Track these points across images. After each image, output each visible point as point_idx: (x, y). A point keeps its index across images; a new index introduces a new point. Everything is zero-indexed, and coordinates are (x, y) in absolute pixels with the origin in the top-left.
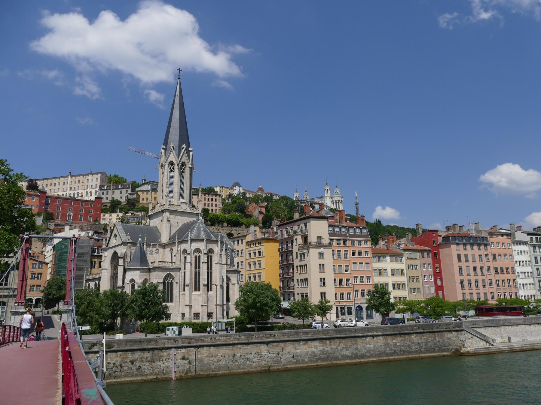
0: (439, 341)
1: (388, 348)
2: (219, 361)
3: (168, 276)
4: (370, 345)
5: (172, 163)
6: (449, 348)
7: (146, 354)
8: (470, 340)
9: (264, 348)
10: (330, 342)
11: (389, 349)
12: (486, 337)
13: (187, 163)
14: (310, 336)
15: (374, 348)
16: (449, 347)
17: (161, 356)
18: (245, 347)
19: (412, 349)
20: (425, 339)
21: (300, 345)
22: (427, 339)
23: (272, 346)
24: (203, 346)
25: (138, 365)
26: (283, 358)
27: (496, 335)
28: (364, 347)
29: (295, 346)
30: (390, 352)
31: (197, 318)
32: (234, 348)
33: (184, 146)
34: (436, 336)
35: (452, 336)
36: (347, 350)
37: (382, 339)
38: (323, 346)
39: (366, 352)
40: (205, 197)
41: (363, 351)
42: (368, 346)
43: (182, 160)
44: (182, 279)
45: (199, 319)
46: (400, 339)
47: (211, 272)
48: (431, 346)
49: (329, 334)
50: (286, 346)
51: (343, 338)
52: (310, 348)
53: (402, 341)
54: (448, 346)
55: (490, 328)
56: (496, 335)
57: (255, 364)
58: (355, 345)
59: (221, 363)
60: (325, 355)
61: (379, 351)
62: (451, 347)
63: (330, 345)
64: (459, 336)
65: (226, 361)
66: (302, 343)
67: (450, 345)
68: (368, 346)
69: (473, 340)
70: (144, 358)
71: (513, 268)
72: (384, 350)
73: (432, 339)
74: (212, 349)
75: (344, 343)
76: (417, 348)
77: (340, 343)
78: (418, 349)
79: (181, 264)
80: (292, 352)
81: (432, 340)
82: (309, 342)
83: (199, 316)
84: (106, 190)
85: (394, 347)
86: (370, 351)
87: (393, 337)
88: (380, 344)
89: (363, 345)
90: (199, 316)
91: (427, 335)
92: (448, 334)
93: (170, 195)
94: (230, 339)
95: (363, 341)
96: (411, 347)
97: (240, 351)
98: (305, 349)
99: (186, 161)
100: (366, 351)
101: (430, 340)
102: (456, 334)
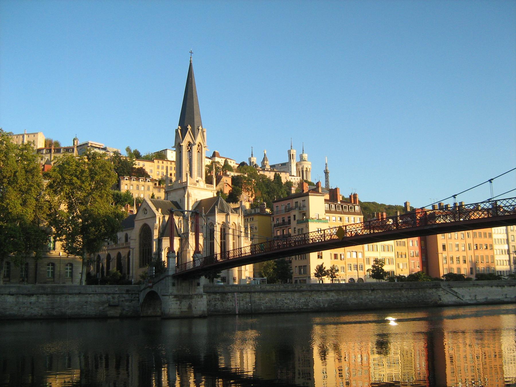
7: (218, 296)
9: (296, 295)
12: (458, 294)
17: (228, 298)
18: (283, 294)
20: (412, 293)
24: (254, 292)
25: (213, 303)
36: (355, 299)
37: (380, 292)
40: (158, 164)
42: (370, 297)
44: (209, 249)
49: (342, 287)
51: (352, 290)
57: (291, 306)
59: (268, 304)
61: (378, 301)
63: (343, 296)
65: (271, 303)
66: (323, 293)
68: (370, 297)
70: (217, 299)
71: (491, 246)
72: (381, 300)
74: (262, 295)
79: (208, 235)
81: (417, 294)
82: (328, 293)
83: (225, 280)
84: (46, 153)
85: (389, 298)
91: (414, 291)
94: (273, 288)
97: (281, 297)
100: (368, 300)
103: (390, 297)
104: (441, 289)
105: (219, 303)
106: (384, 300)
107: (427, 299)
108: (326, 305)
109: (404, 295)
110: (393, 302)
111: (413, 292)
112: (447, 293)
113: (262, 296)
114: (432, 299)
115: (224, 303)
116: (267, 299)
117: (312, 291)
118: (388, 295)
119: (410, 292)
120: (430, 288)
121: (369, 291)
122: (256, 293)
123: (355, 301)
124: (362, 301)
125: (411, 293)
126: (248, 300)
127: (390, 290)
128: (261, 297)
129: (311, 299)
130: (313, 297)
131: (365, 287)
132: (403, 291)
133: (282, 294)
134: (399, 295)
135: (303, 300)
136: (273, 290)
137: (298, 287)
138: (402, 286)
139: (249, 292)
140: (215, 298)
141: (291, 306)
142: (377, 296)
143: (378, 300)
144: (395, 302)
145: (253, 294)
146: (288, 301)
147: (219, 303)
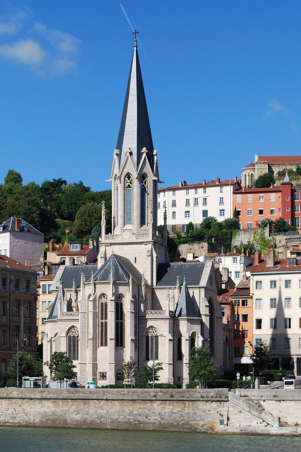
0: (188, 413)
4: (102, 410)
5: (129, 176)
6: (199, 424)
8: (237, 416)
10: (63, 403)
11: (122, 417)
14: (45, 395)
15: (106, 414)
16: (199, 422)
21: (35, 404)
22: (173, 409)
23: (12, 403)
28: (95, 411)
29: (29, 404)
30: (123, 420)
34: (187, 406)
36: (78, 413)
37: (118, 404)
39: (96, 418)
42: (100, 411)
46: (139, 406)
48: (176, 419)
49: (63, 395)
50: (23, 404)
52: (43, 408)
53: (140, 408)
54: (198, 421)
58: (86, 409)
60: (55, 416)
61: (111, 418)
62: (203, 423)
63: (63, 407)
64: (219, 409)
68: (100, 411)
69: (242, 414)
72: (117, 417)
73: (180, 410)
75: (76, 406)
76: (155, 420)
77: (72, 405)
78: (157, 420)
81: (179, 411)
82: (43, 402)
85: (129, 415)
86: (102, 417)
87: (131, 402)
88: (114, 411)
89: (96, 410)
90: (106, 376)
91: (175, 405)
95: (96, 406)
98: (39, 408)
99: (130, 172)
102: (216, 406)
103: (131, 413)
106: (121, 417)
107: (197, 421)
108: (37, 420)
109: (156, 411)
112: (241, 412)
119: (167, 407)
123: (78, 417)
124: (87, 416)
129: (21, 410)
131: (95, 395)
135: (10, 411)
137: (7, 393)
142: (112, 410)
143: (112, 417)
144: (136, 422)
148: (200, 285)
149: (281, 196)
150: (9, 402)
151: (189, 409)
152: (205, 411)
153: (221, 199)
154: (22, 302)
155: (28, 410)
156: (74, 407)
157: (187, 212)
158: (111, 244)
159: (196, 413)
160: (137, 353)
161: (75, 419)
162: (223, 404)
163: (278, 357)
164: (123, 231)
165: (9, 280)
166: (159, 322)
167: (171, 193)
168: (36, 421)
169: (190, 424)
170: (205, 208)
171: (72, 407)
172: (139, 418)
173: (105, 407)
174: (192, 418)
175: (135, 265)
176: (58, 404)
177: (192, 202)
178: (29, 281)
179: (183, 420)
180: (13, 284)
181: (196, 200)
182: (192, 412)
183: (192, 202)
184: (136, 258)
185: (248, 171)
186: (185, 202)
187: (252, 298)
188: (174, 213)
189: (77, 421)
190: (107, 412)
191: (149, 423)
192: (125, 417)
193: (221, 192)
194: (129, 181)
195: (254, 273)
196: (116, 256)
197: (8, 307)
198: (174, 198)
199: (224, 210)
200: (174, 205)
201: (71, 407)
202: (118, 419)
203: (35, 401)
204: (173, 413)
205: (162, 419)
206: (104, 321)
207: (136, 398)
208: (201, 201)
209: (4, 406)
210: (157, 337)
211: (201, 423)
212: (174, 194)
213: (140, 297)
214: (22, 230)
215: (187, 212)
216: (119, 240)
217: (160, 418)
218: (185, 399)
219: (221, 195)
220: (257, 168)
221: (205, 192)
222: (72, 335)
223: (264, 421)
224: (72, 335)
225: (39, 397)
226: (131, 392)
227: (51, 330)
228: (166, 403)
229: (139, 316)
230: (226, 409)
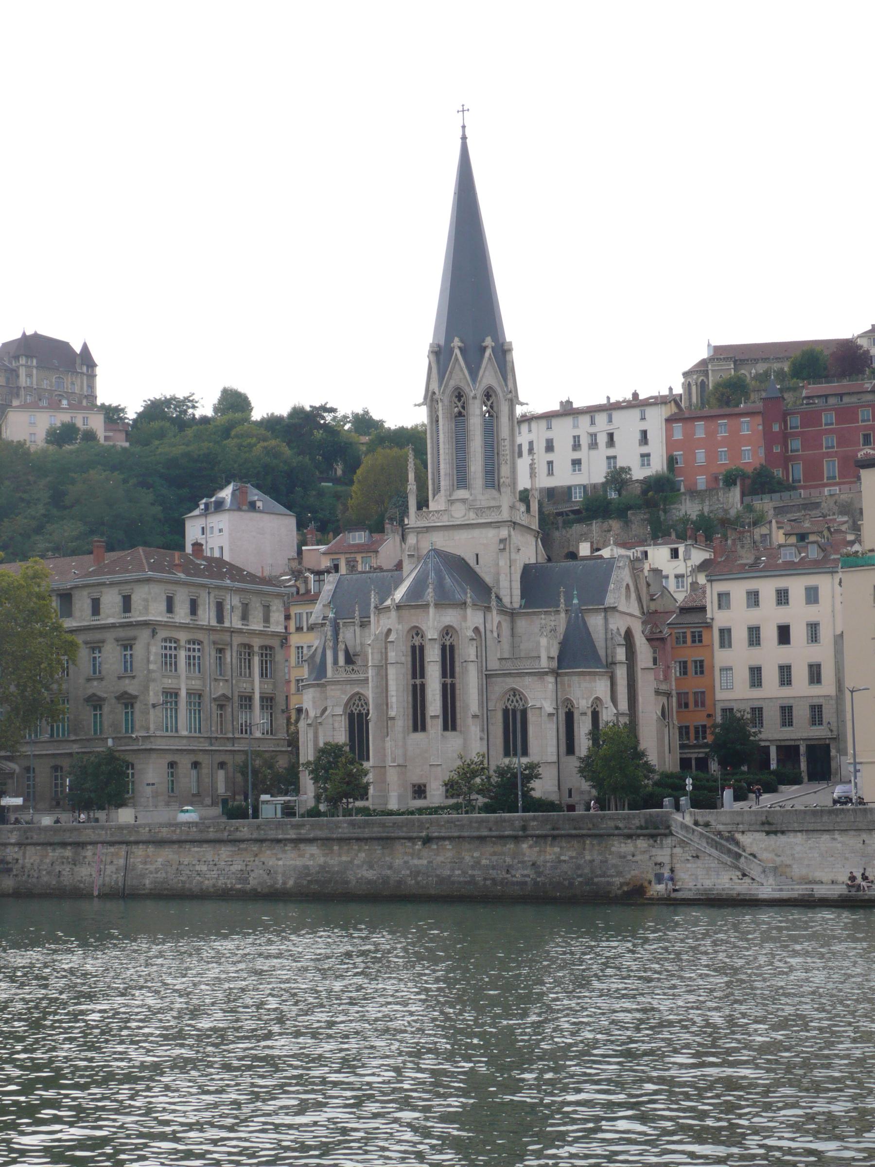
0: (592, 861)
1: (459, 869)
2: (157, 871)
3: (360, 700)
4: (419, 858)
8: (689, 865)
13: (466, 387)
17: (85, 857)
18: (196, 849)
19: (515, 876)
21: (284, 852)
22: (561, 855)
24: (137, 843)
26: (253, 875)
27: (847, 859)
28: (406, 862)
29: (274, 851)
30: (462, 879)
31: (420, 798)
32: (181, 850)
33: (456, 339)
34: (587, 847)
35: (632, 849)
36: (371, 867)
37: (449, 847)
38: (326, 855)
39: (408, 876)
41: (403, 872)
42: (416, 862)
43: (452, 383)
45: (367, 799)
46: (492, 850)
47: (423, 686)
48: (566, 873)
49: (340, 830)
53: (494, 854)
54: (612, 876)
55: (826, 837)
56: (847, 859)
57: (207, 882)
58: (387, 859)
59: (159, 875)
60: (325, 875)
61: (437, 876)
62: (622, 880)
63: (340, 855)
64: (654, 851)
65: (167, 873)
67: (620, 874)
68: (416, 862)
69: (699, 863)
72: (448, 873)
73: (574, 854)
74: (151, 849)
76: (526, 876)
77: (359, 851)
80: (271, 863)
81: (571, 858)
82: (302, 846)
85: (473, 868)
86: (418, 873)
89: (406, 858)
92: (623, 845)
93: (462, 480)
94: (175, 831)
95: (407, 850)
96: (513, 872)
98: (293, 859)
99: (462, 385)
100: (408, 872)
101: (566, 858)
102: (646, 845)
103: (477, 864)
104: (668, 841)
105: (66, 869)
106: (457, 872)
107: (608, 877)
108: (291, 883)
109: (526, 859)
110: (485, 879)
111: (561, 848)
112: (697, 857)
113: (150, 854)
114: (628, 877)
115: (76, 869)
116: (160, 860)
117: (262, 841)
118: (472, 857)
120: (629, 836)
121: (414, 844)
122: (141, 846)
123: (370, 874)
124: (389, 872)
125: (551, 852)
126: (122, 862)
127: (482, 839)
128: (148, 856)
130: (262, 859)
132: (525, 846)
133: (193, 849)
134: (508, 860)
135: (237, 867)
136: (175, 837)
137: (230, 831)
138: (524, 828)
139: (128, 843)
140: (63, 857)
141: (207, 882)
142: (440, 859)
143: (438, 872)
144: (488, 882)
145: (134, 849)
146: (204, 868)
147: (66, 869)
148: (606, 605)
149: (761, 422)
150: (234, 849)
151: (591, 854)
152: (625, 857)
153: (644, 433)
154: (256, 649)
155: (271, 862)
156: (363, 855)
157: (576, 463)
158: (428, 529)
159: (606, 861)
160: (485, 742)
161: (366, 878)
162: (661, 841)
163: (767, 744)
164: (451, 502)
165: (229, 607)
166: (528, 680)
167: (543, 424)
168: (288, 886)
169: (596, 884)
170: (611, 452)
171: (359, 855)
172: (493, 873)
173: (425, 853)
174: (599, 872)
175: (477, 569)
176: (332, 850)
177: (585, 441)
178: (268, 607)
179: (580, 876)
180: (238, 613)
181: (593, 436)
182: (598, 858)
183: (585, 441)
184: (477, 555)
185: (695, 377)
186: (572, 443)
187: (709, 626)
188: (550, 463)
189: (369, 882)
190: (429, 862)
191: (513, 883)
192: (464, 873)
193: (643, 418)
194: (459, 404)
195: (713, 578)
196: (438, 553)
197: (229, 660)
198: (549, 435)
199: (648, 455)
200: (549, 447)
201: (357, 855)
202: (450, 876)
203: (285, 845)
204: (560, 861)
205: (539, 874)
206: (418, 681)
207: (485, 833)
208: (602, 439)
209: (224, 856)
210: (524, 712)
211: (617, 880)
212: (549, 428)
213: (488, 633)
214: (252, 506)
215: (576, 463)
216: (445, 521)
217: (536, 873)
218: (584, 832)
219: (643, 426)
220: (713, 370)
221: (610, 420)
222: (356, 712)
223: (744, 875)
224: (356, 712)
225: (294, 836)
226: (476, 822)
227: (314, 702)
228: (546, 843)
229: (486, 670)
230: (667, 851)
